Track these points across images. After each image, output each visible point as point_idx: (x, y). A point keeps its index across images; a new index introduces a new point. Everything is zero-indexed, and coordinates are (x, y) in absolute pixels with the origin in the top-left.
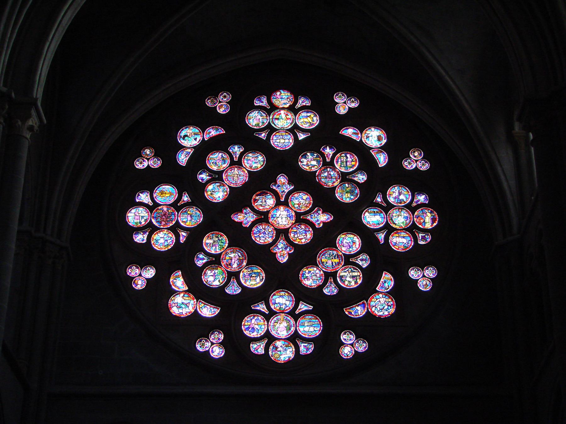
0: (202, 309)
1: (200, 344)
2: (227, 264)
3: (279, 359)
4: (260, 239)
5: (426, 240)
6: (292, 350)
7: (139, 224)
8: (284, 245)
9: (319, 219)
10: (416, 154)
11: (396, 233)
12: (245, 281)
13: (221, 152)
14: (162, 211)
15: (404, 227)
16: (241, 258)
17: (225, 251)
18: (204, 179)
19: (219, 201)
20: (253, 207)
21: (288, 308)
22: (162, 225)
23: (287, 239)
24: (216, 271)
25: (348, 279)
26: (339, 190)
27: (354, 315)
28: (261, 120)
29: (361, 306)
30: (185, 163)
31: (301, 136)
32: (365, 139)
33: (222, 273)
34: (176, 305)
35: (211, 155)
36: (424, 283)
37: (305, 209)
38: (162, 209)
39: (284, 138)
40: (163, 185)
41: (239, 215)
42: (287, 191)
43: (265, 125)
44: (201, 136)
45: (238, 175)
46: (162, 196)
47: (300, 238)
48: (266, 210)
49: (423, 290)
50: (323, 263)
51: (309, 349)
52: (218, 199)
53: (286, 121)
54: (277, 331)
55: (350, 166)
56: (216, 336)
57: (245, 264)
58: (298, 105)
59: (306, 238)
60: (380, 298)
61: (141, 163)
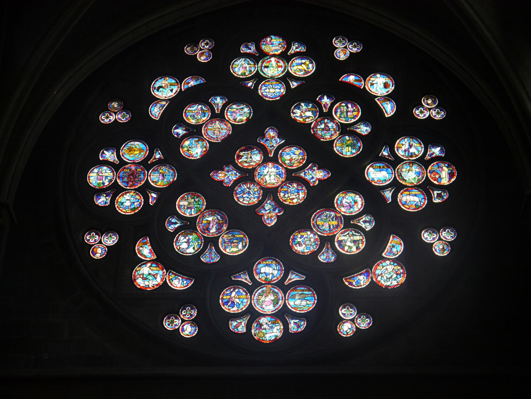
0: (173, 281)
1: (169, 321)
3: (264, 339)
4: (244, 200)
5: (443, 198)
6: (279, 328)
7: (102, 185)
8: (272, 206)
9: (314, 176)
10: (430, 102)
11: (405, 191)
12: (225, 248)
13: (200, 104)
14: (130, 170)
15: (415, 183)
16: (221, 222)
18: (180, 134)
20: (237, 164)
21: (275, 278)
22: (128, 185)
23: (276, 200)
24: (191, 237)
25: (349, 244)
26: (338, 143)
28: (248, 68)
29: (364, 275)
30: (158, 117)
31: (294, 85)
33: (197, 239)
34: (142, 276)
35: (189, 107)
36: (441, 247)
37: (297, 165)
40: (132, 141)
41: (219, 173)
42: (276, 146)
43: (253, 74)
44: (178, 87)
45: (219, 129)
46: (130, 153)
47: (291, 197)
48: (251, 168)
49: (439, 255)
50: (318, 226)
51: (300, 327)
52: (196, 155)
53: (276, 69)
54: (262, 305)
55: (351, 116)
56: (188, 313)
57: (225, 228)
58: (291, 51)
60: (388, 265)
61: (107, 117)
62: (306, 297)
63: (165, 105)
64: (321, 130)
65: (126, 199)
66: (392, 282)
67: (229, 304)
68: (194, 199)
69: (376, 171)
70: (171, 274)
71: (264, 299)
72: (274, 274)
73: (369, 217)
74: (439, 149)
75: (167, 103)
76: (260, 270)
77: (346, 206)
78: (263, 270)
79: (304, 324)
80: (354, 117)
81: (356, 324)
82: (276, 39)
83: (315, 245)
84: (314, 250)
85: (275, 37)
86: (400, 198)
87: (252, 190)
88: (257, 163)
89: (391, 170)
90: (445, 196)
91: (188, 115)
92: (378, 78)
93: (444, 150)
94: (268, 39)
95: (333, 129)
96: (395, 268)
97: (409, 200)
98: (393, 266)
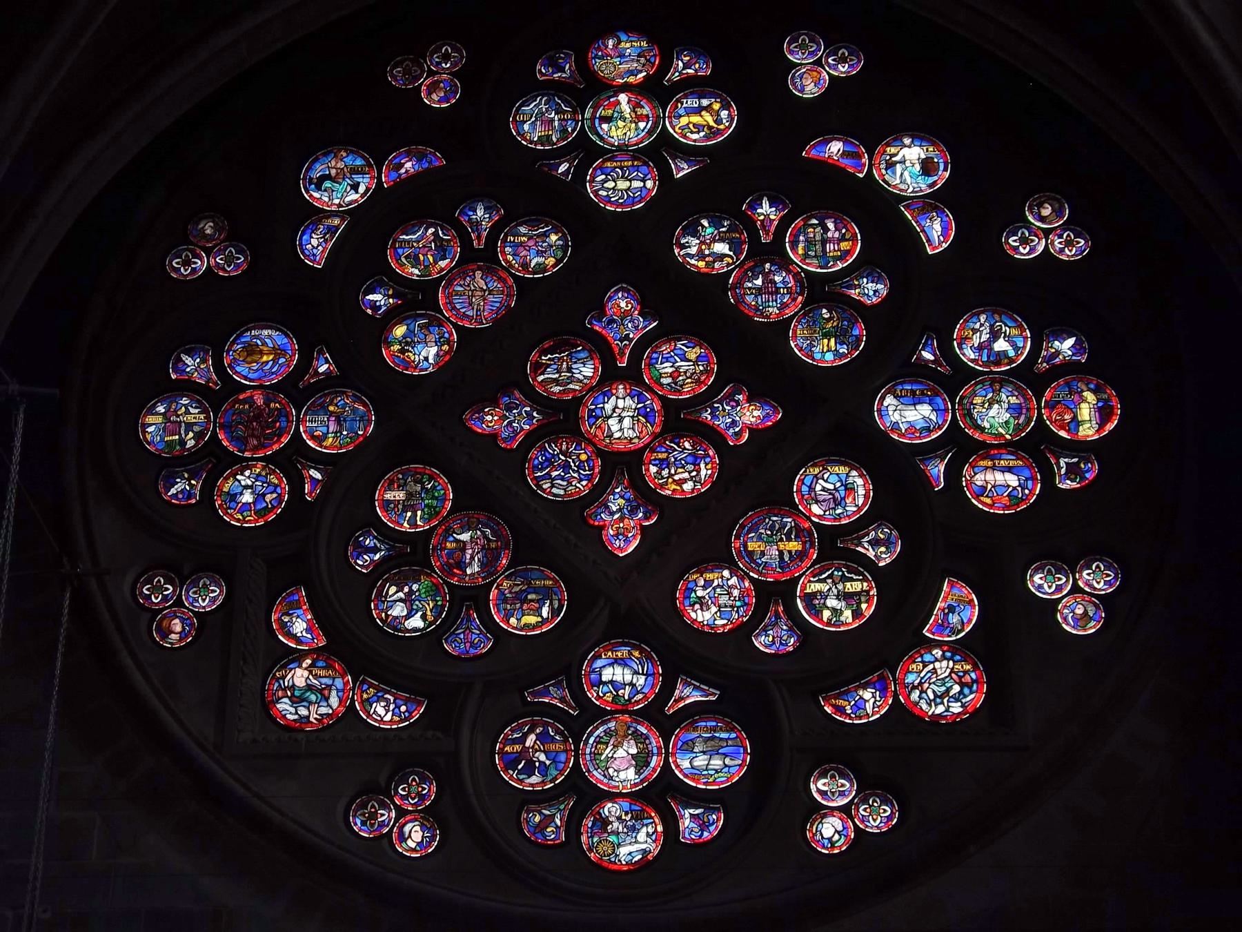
1: (363, 815)
2: (447, 564)
3: (613, 860)
4: (553, 486)
5: (1083, 478)
7: (178, 448)
8: (628, 500)
9: (738, 419)
10: (1046, 211)
15: (1008, 437)
16: (493, 545)
17: (444, 524)
18: (380, 307)
19: (426, 369)
20: (533, 387)
21: (640, 696)
24: (415, 587)
26: (800, 327)
27: (853, 716)
31: (682, 170)
32: (884, 172)
36: (1079, 611)
38: (250, 401)
39: (629, 175)
41: (488, 414)
44: (372, 178)
46: (249, 359)
47: (676, 477)
50: (751, 554)
51: (708, 827)
54: (607, 769)
55: (835, 254)
59: (697, 479)
60: (937, 660)
61: (187, 263)
62: (722, 747)
63: (337, 228)
64: (754, 291)
65: (243, 483)
66: (949, 707)
67: (520, 767)
68: (423, 484)
69: (902, 404)
70: (365, 687)
71: (613, 752)
72: (637, 685)
73: (886, 530)
74: (1071, 342)
75: (343, 220)
76: (601, 675)
77: (824, 501)
78: (607, 675)
79: (718, 819)
80: (845, 254)
81: (856, 820)
82: (632, 41)
83: (742, 606)
84: (740, 619)
85: (629, 37)
86: (969, 478)
87: (573, 460)
88: (586, 384)
89: (944, 400)
90: (1087, 471)
91: (401, 254)
92: (905, 146)
93: (1086, 345)
94: (611, 40)
95: (785, 290)
96: (956, 667)
97: (993, 483)
98: (951, 663)
